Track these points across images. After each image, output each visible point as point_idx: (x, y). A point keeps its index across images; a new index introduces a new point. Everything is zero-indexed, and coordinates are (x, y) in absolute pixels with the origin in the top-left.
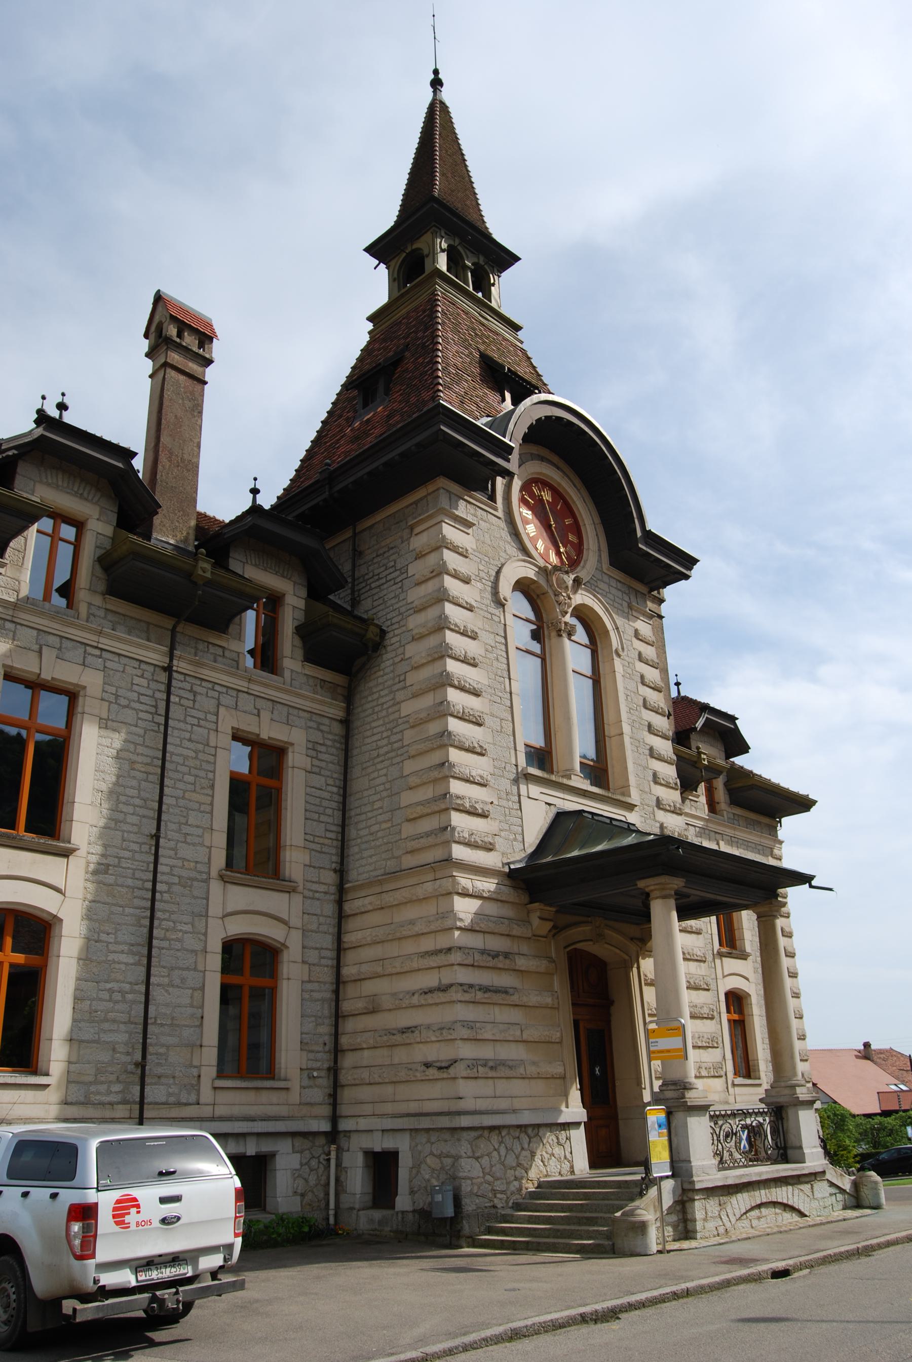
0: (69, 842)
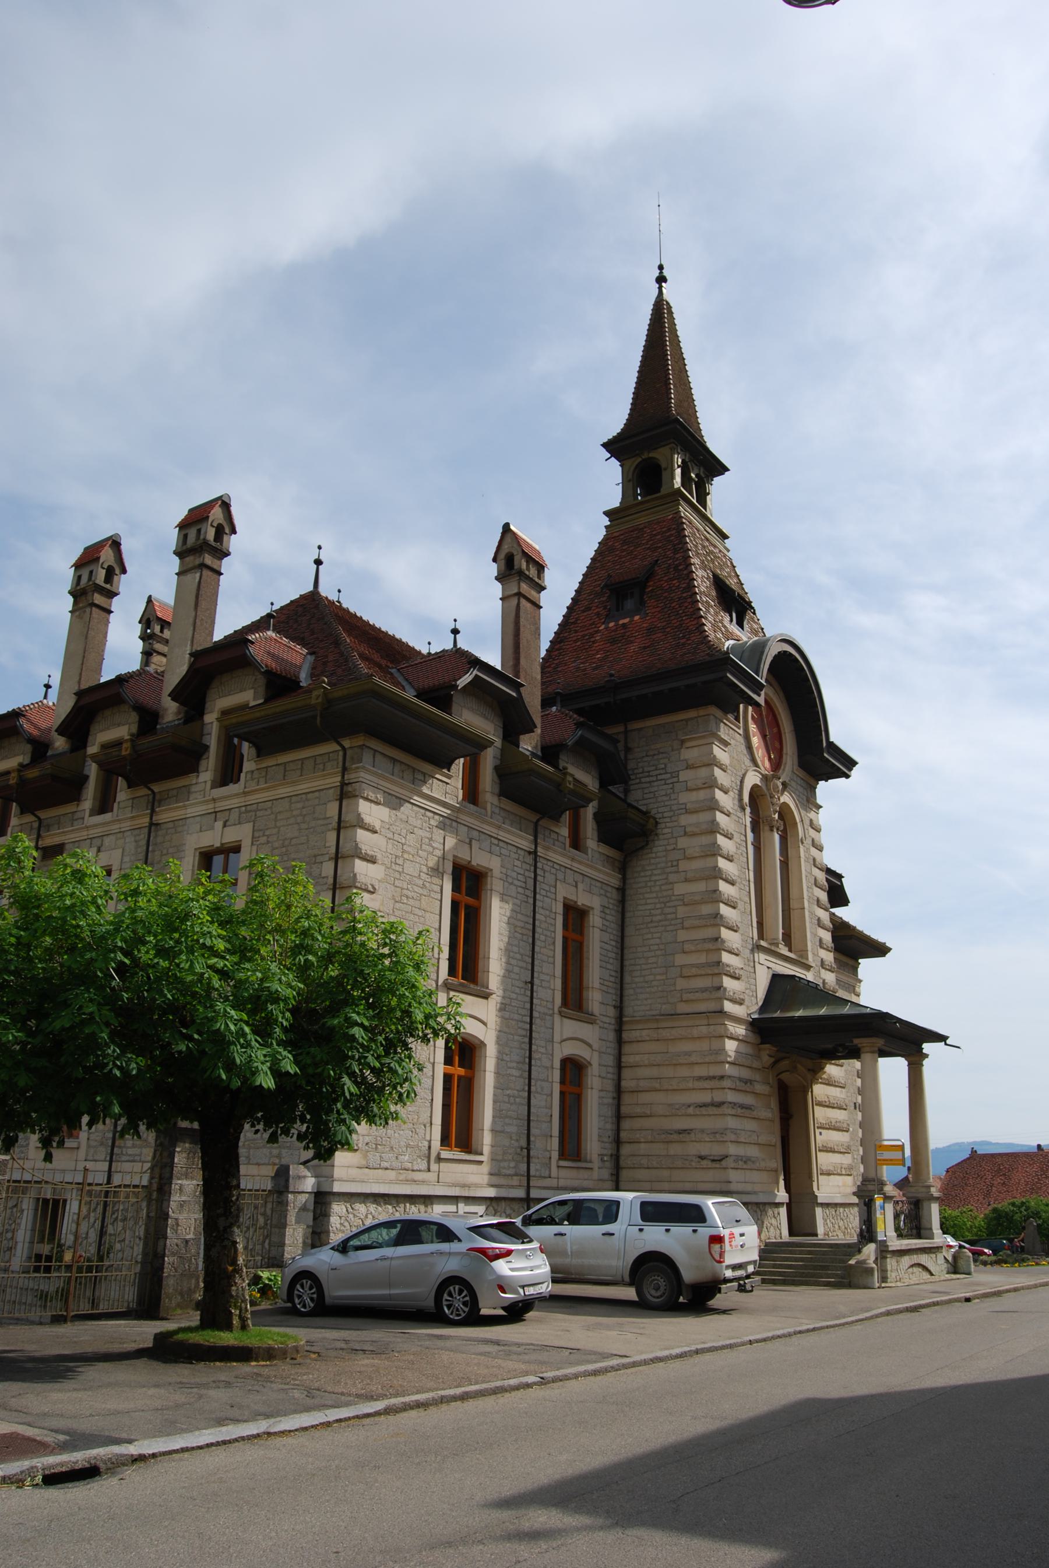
0: (487, 988)
